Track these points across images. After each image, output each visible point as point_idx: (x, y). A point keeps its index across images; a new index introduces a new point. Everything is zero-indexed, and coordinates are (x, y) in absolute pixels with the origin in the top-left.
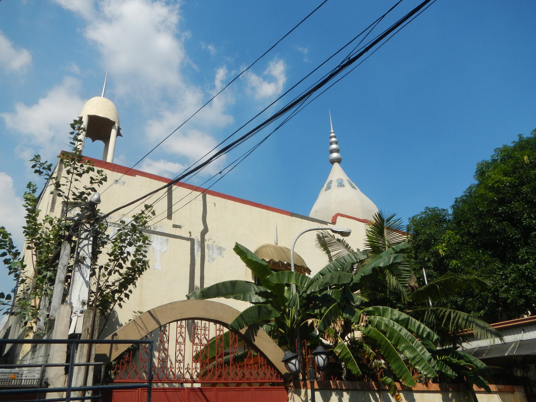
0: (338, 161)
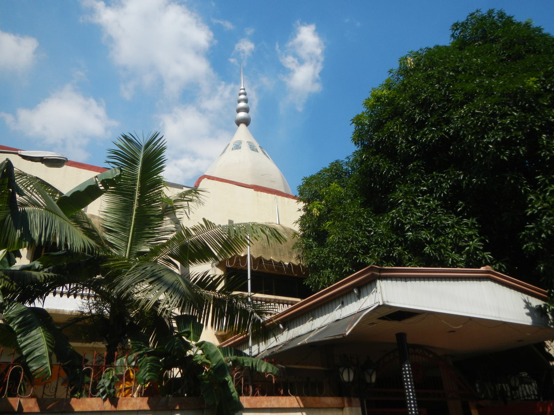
0: (246, 122)
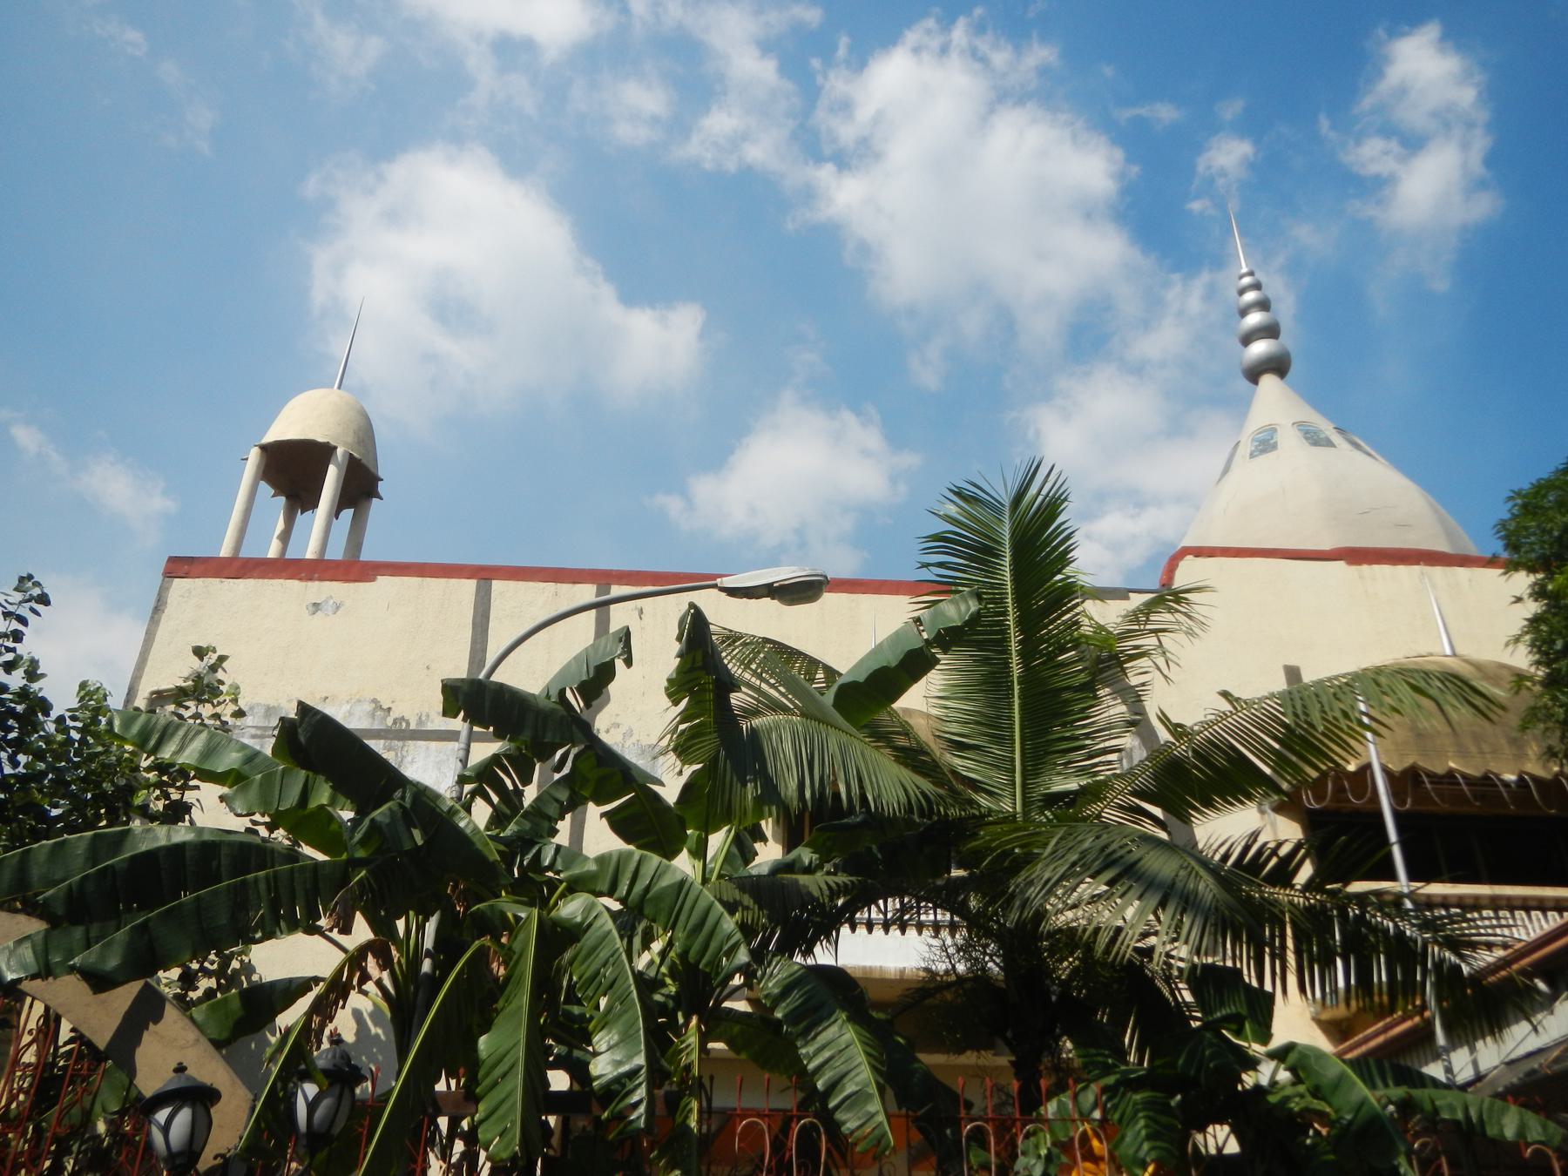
0: (1278, 366)
